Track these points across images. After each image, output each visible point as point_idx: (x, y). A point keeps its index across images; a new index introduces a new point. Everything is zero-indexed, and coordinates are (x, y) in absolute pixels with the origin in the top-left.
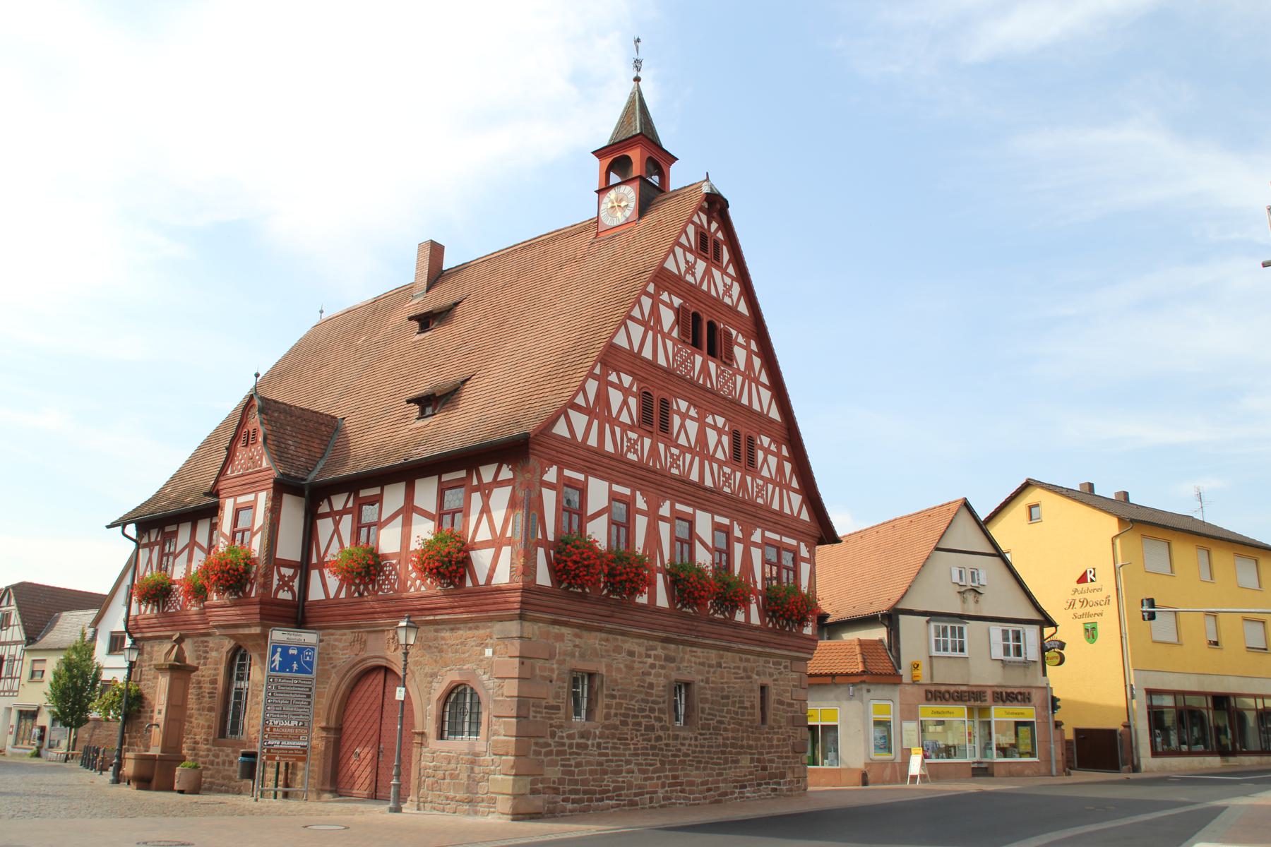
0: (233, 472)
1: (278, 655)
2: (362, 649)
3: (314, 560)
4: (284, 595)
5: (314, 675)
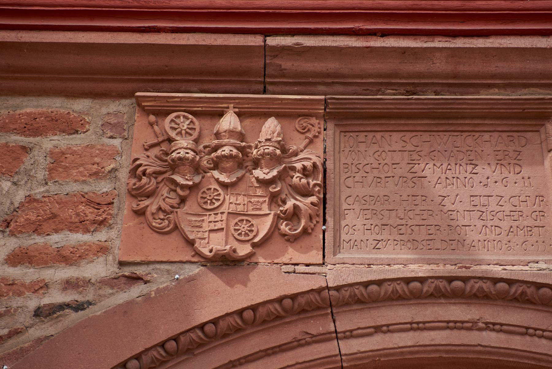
2: (293, 230)
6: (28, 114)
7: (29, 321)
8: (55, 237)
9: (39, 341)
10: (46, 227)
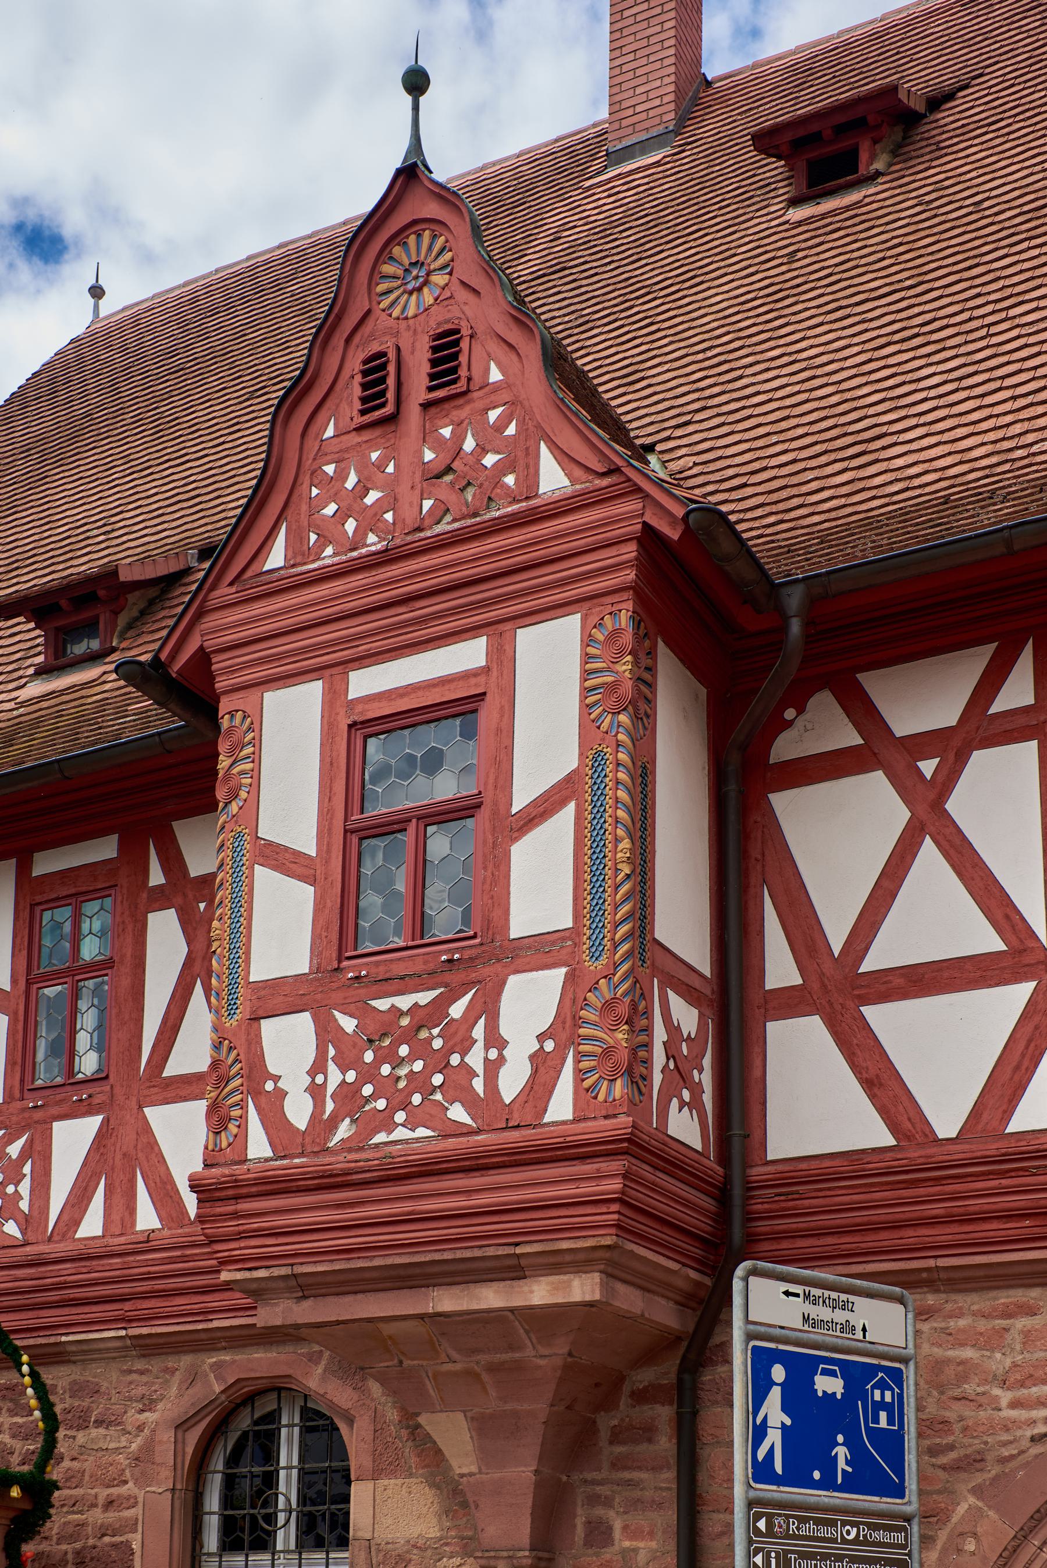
0: (297, 551)
1: (775, 1395)
3: (781, 969)
4: (685, 1127)
5: (910, 1503)
6: (1003, 1304)
7: (1028, 1444)
8: (1034, 1389)
9: (1036, 1456)
10: (1028, 1383)
